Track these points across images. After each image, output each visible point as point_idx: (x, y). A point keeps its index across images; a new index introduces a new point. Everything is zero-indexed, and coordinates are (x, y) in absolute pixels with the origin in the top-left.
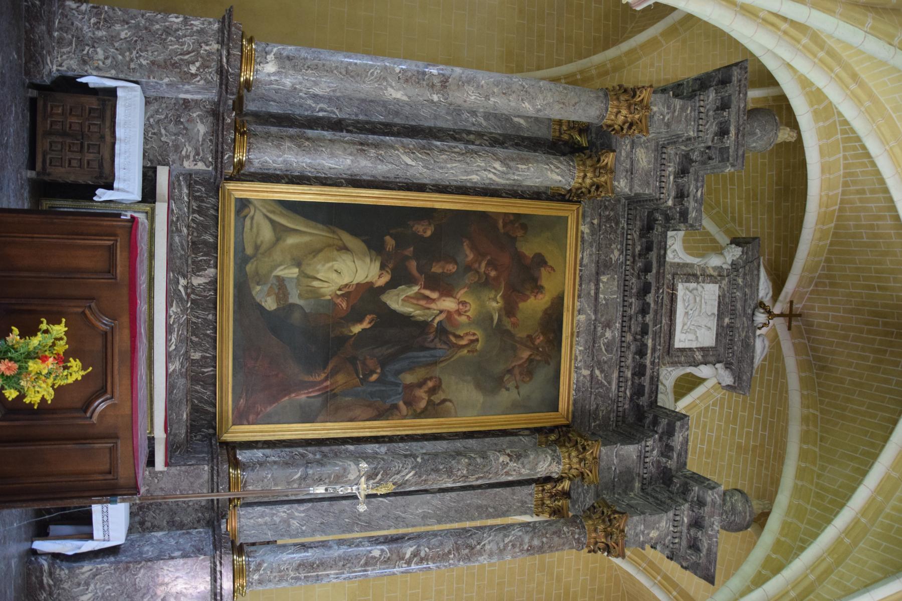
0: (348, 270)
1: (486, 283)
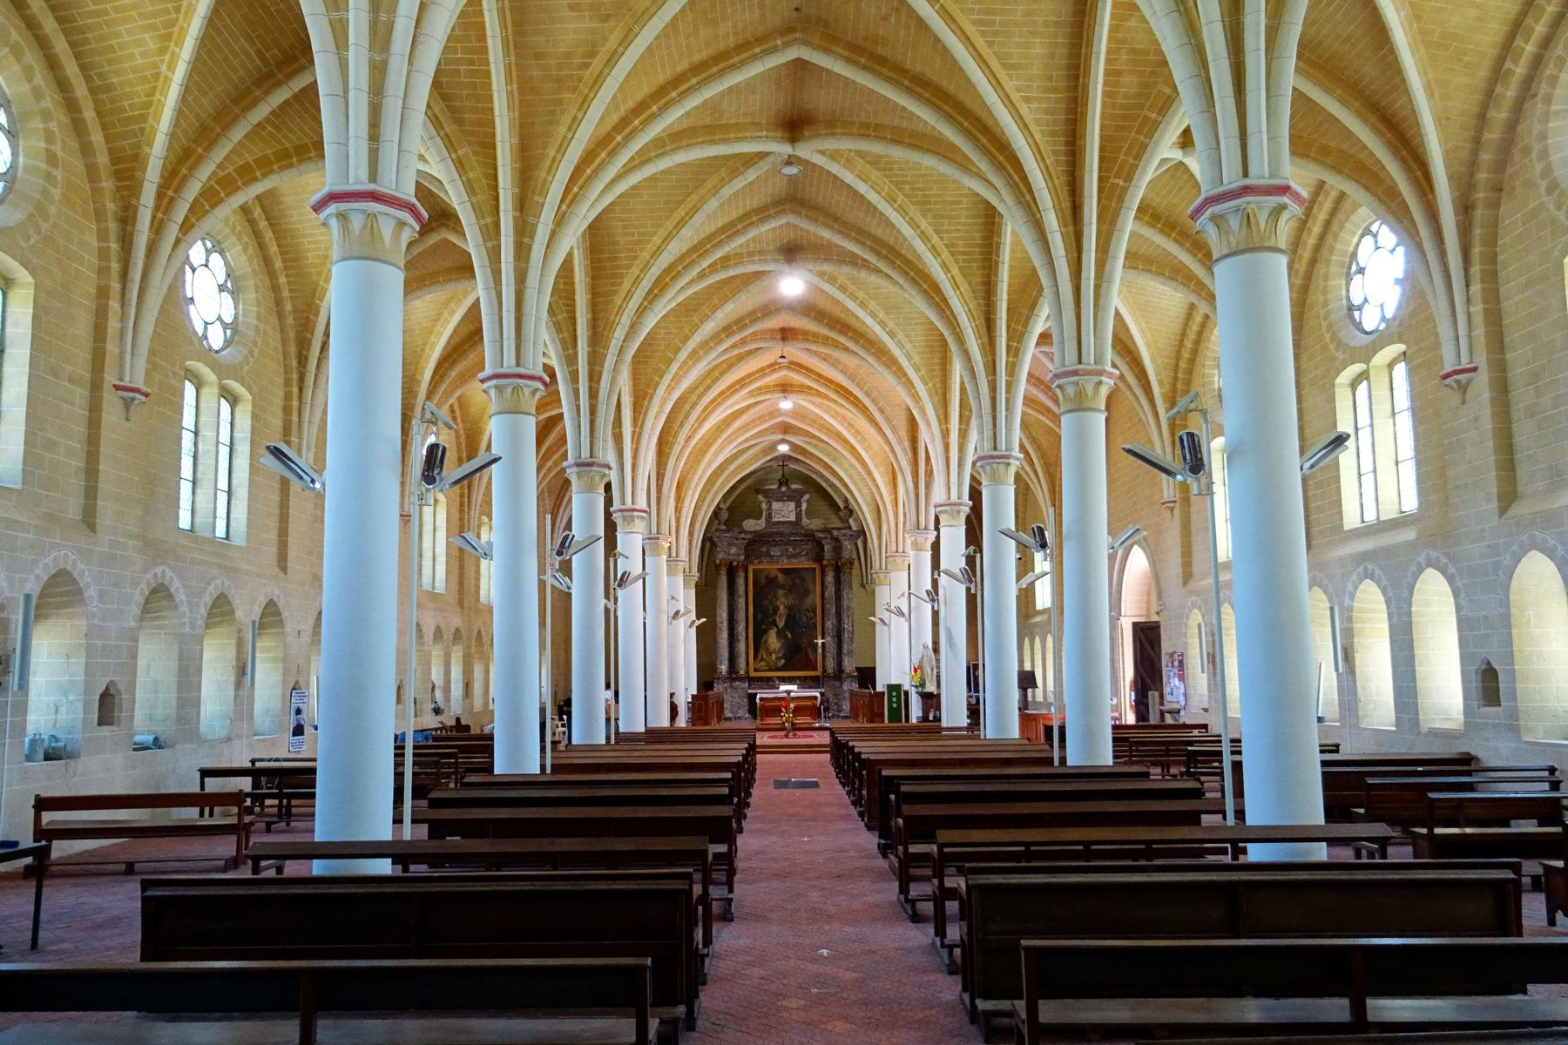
0: (773, 640)
1: (775, 595)
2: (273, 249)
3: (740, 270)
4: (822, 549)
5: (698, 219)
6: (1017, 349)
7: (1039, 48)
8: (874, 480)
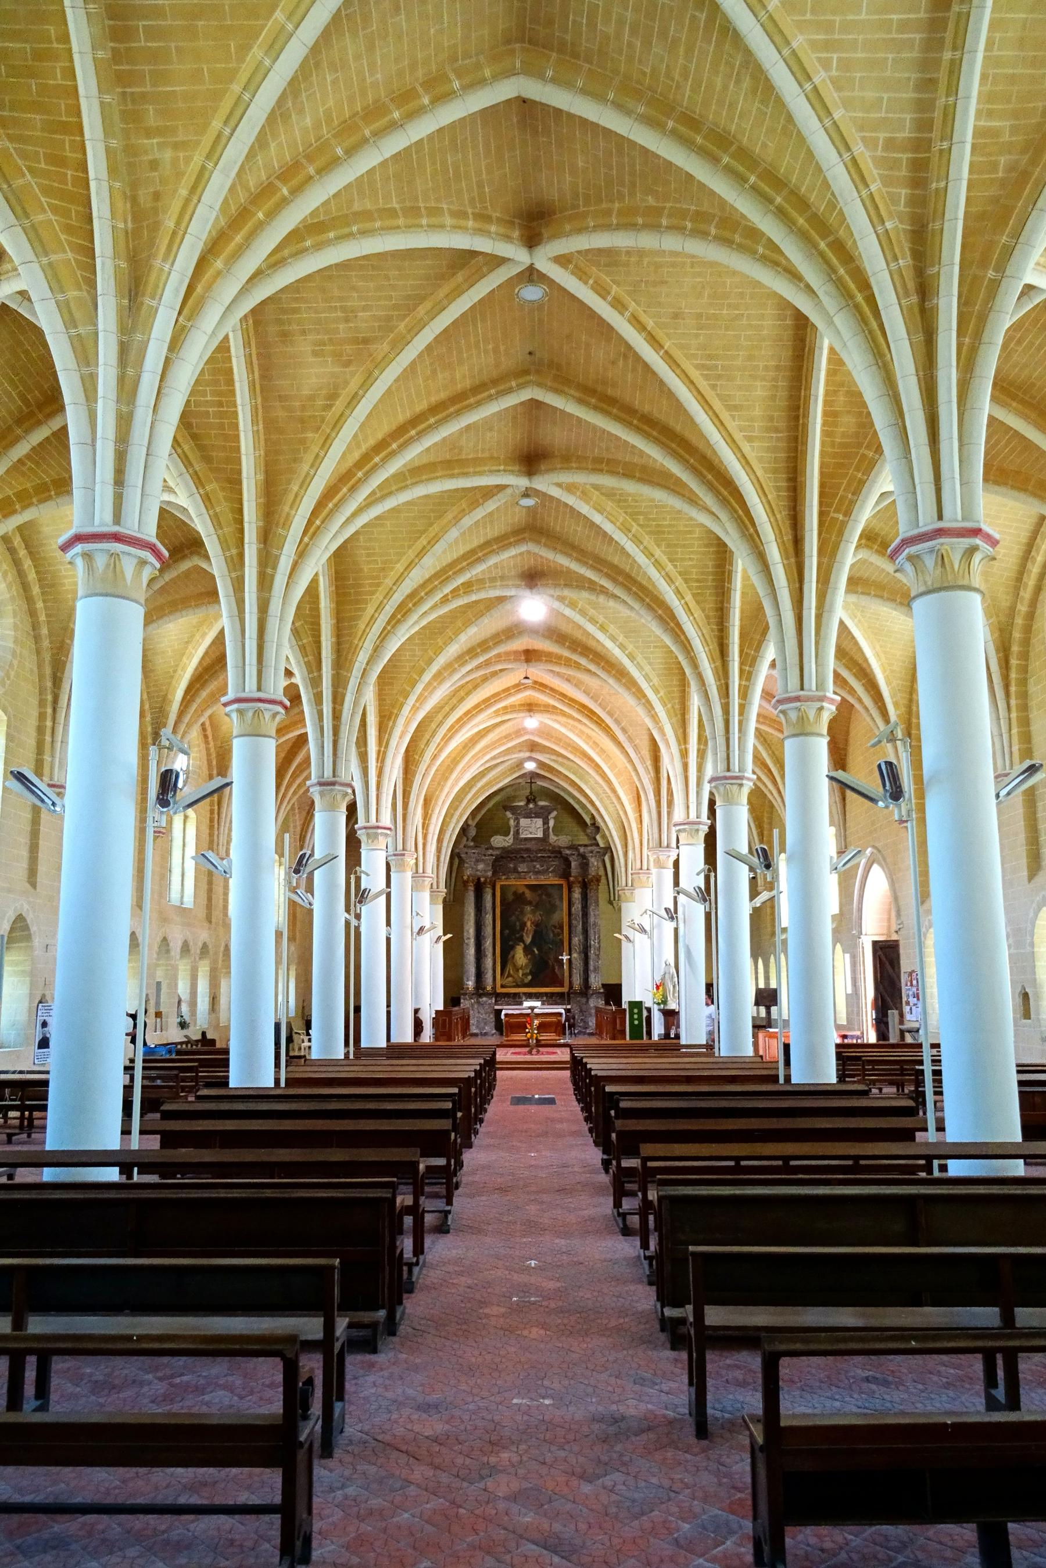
0: (520, 956)
1: (522, 912)
2: (32, 576)
3: (482, 595)
4: (568, 864)
5: (439, 547)
6: (750, 673)
7: (760, 390)
8: (619, 798)
